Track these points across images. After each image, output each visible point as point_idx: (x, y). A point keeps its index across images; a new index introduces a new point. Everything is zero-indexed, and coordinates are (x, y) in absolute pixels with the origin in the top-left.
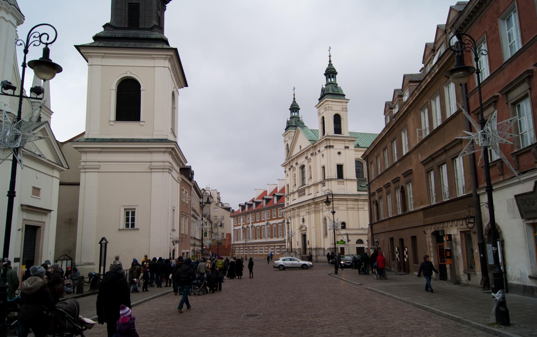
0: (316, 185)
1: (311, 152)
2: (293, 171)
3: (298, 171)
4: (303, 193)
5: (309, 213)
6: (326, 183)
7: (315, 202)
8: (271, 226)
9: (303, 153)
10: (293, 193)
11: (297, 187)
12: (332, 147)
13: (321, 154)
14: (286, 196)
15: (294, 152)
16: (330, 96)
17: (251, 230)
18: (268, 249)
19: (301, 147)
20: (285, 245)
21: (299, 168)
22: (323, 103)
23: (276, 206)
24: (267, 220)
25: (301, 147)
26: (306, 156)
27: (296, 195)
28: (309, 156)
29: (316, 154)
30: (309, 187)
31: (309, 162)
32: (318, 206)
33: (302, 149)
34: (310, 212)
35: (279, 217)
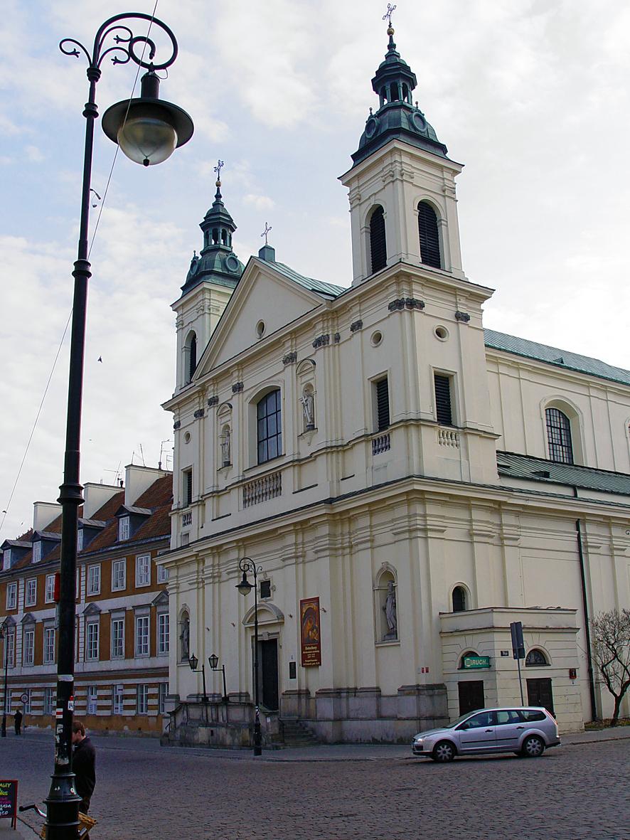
0: (339, 449)
1: (319, 335)
2: (220, 415)
3: (242, 416)
4: (269, 486)
5: (300, 558)
6: (397, 438)
7: (334, 515)
8: (105, 618)
9: (278, 343)
10: (217, 494)
11: (235, 474)
12: (422, 305)
13: (368, 335)
14: (179, 509)
15: (226, 348)
16: (402, 137)
17: (19, 632)
18: (85, 698)
19: (261, 327)
20: (166, 685)
21: (247, 404)
22: (381, 160)
23: (130, 550)
24: (88, 599)
25: (261, 327)
26: (287, 353)
27: (237, 495)
28: (305, 349)
29: (337, 338)
30: (299, 463)
31: (300, 373)
32: (346, 530)
33: (267, 332)
34: (304, 556)
35: (138, 585)
